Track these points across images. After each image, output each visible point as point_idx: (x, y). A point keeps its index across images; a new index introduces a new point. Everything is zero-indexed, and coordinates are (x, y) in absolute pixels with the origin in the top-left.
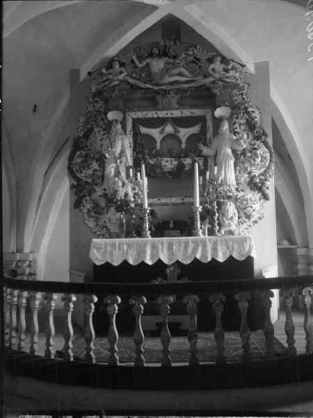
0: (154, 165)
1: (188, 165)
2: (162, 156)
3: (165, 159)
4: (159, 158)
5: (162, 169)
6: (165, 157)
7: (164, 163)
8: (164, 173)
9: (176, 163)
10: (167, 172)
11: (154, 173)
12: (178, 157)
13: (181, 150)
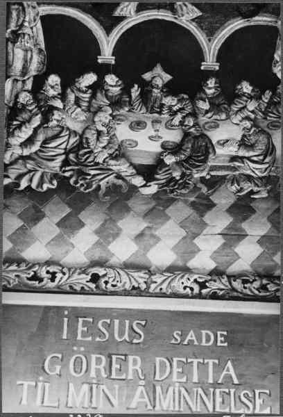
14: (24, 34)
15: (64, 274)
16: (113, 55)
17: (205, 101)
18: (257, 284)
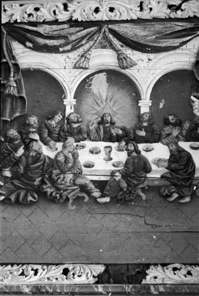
0: (54, 163)
1: (158, 162)
2: (80, 135)
3: (89, 144)
4: (71, 140)
5: (78, 174)
7: (84, 157)
8: (83, 188)
9: (123, 157)
10: (101, 185)
11: (54, 183)
12: (128, 137)
13: (140, 117)
14: (10, 86)
15: (44, 270)
16: (74, 98)
17: (142, 130)
18: (184, 271)
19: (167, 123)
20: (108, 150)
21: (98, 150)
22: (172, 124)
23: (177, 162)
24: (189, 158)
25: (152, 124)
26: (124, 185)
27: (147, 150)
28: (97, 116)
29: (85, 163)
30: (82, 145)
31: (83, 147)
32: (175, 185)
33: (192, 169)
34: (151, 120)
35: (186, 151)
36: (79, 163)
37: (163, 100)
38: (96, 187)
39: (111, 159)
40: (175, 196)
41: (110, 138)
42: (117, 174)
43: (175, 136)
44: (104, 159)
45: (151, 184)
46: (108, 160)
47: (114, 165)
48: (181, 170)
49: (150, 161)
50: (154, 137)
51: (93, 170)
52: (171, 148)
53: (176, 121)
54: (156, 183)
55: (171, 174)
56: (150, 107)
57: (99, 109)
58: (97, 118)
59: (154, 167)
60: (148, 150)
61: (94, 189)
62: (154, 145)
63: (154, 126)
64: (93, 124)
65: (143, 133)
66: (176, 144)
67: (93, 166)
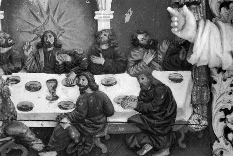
1: (124, 101)
3: (26, 77)
6: (23, 68)
7: (18, 95)
8: (19, 139)
9: (70, 94)
10: (43, 133)
12: (79, 67)
17: (99, 56)
19: (136, 44)
20: (53, 84)
21: (38, 85)
22: (142, 46)
23: (151, 100)
24: (168, 93)
25: (114, 47)
26: (74, 134)
27: (109, 84)
28: (35, 36)
29: (20, 103)
30: (16, 78)
31: (17, 81)
32: (146, 132)
33: (172, 112)
34: (112, 42)
35: (163, 85)
36: (12, 103)
37: (130, 10)
38: (37, 136)
39: (57, 98)
40: (148, 148)
41: (55, 68)
42: (65, 120)
43: (147, 63)
44: (46, 98)
45: (114, 131)
46: (53, 100)
47: (60, 107)
48: (156, 112)
49: (112, 100)
50: (117, 65)
51: (31, 114)
52: (142, 81)
53: (149, 42)
54: (121, 130)
55: (143, 119)
56: (112, 22)
57: (37, 24)
58: (34, 39)
59: (117, 108)
60: (110, 83)
61: (33, 141)
62: (118, 77)
63: (116, 49)
64: (29, 47)
65: (100, 60)
66: (149, 75)
67: (31, 108)
